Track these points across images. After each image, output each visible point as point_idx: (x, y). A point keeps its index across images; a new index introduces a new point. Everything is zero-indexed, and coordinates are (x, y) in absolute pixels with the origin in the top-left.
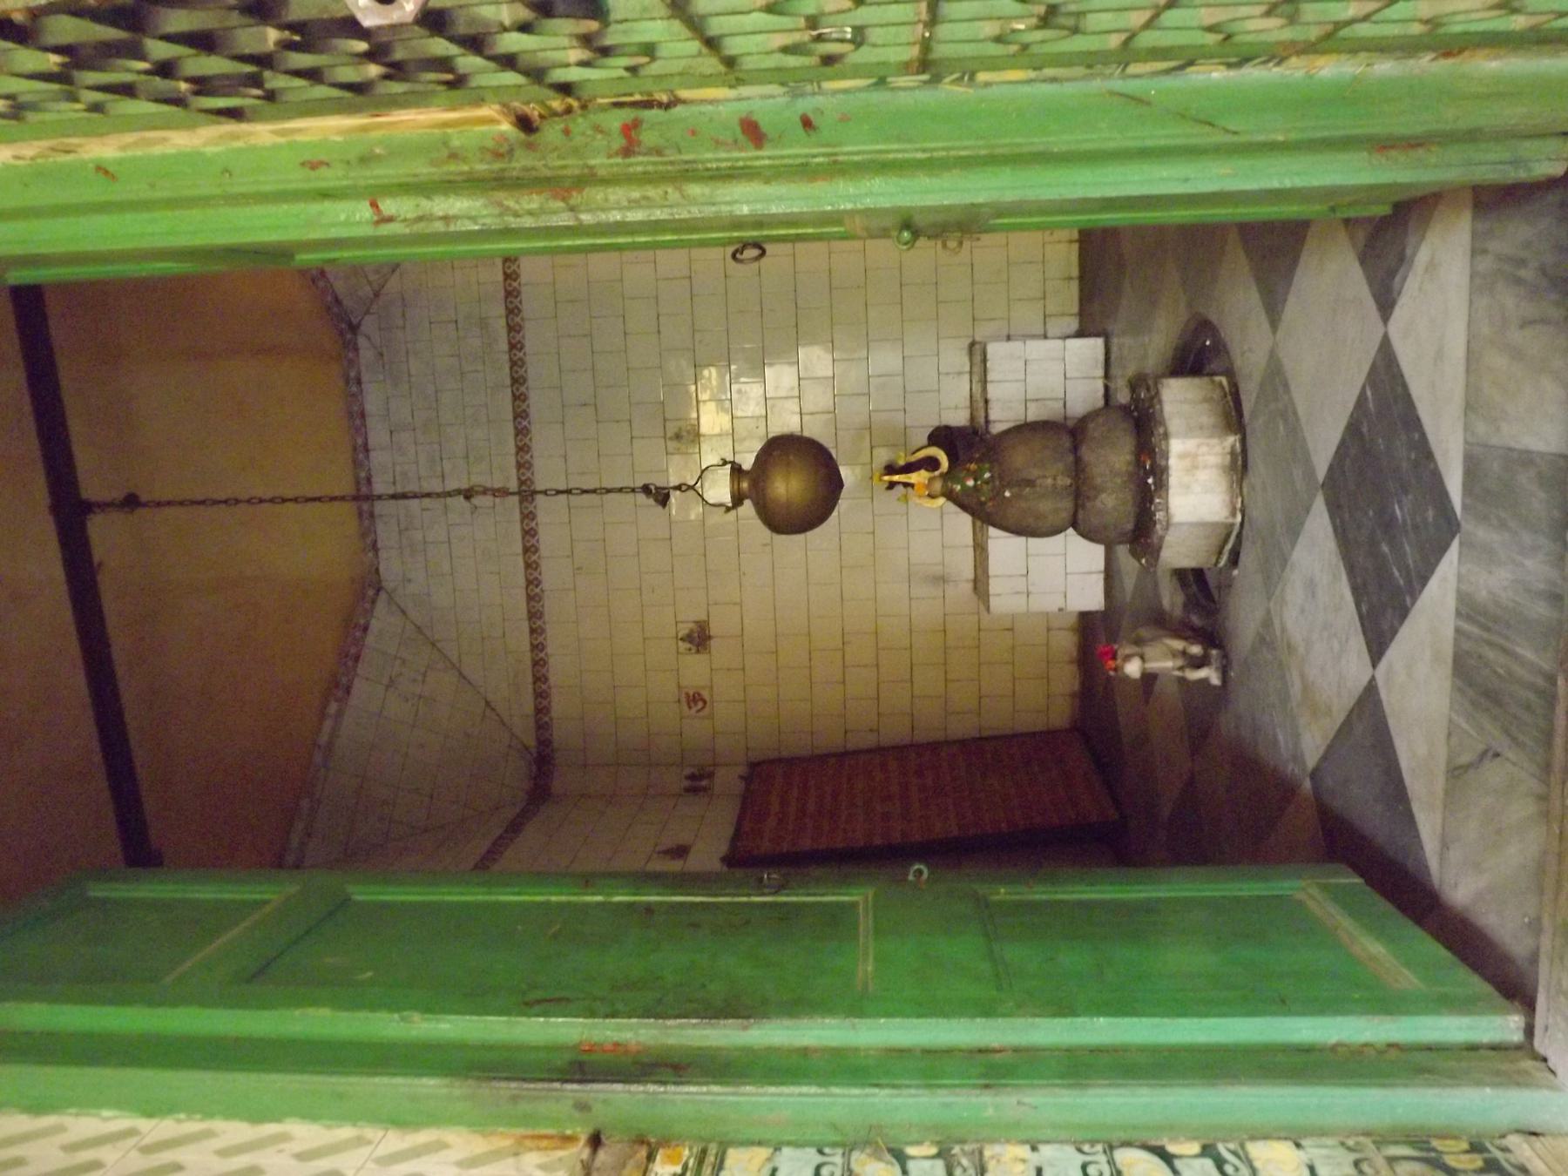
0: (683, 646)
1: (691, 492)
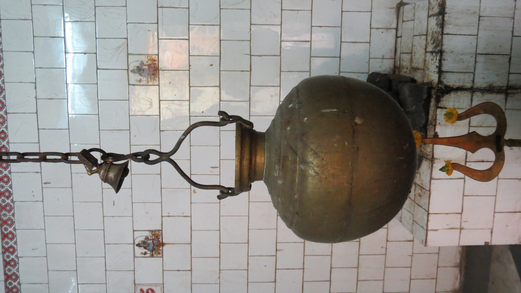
0: (139, 251)
1: (165, 165)
